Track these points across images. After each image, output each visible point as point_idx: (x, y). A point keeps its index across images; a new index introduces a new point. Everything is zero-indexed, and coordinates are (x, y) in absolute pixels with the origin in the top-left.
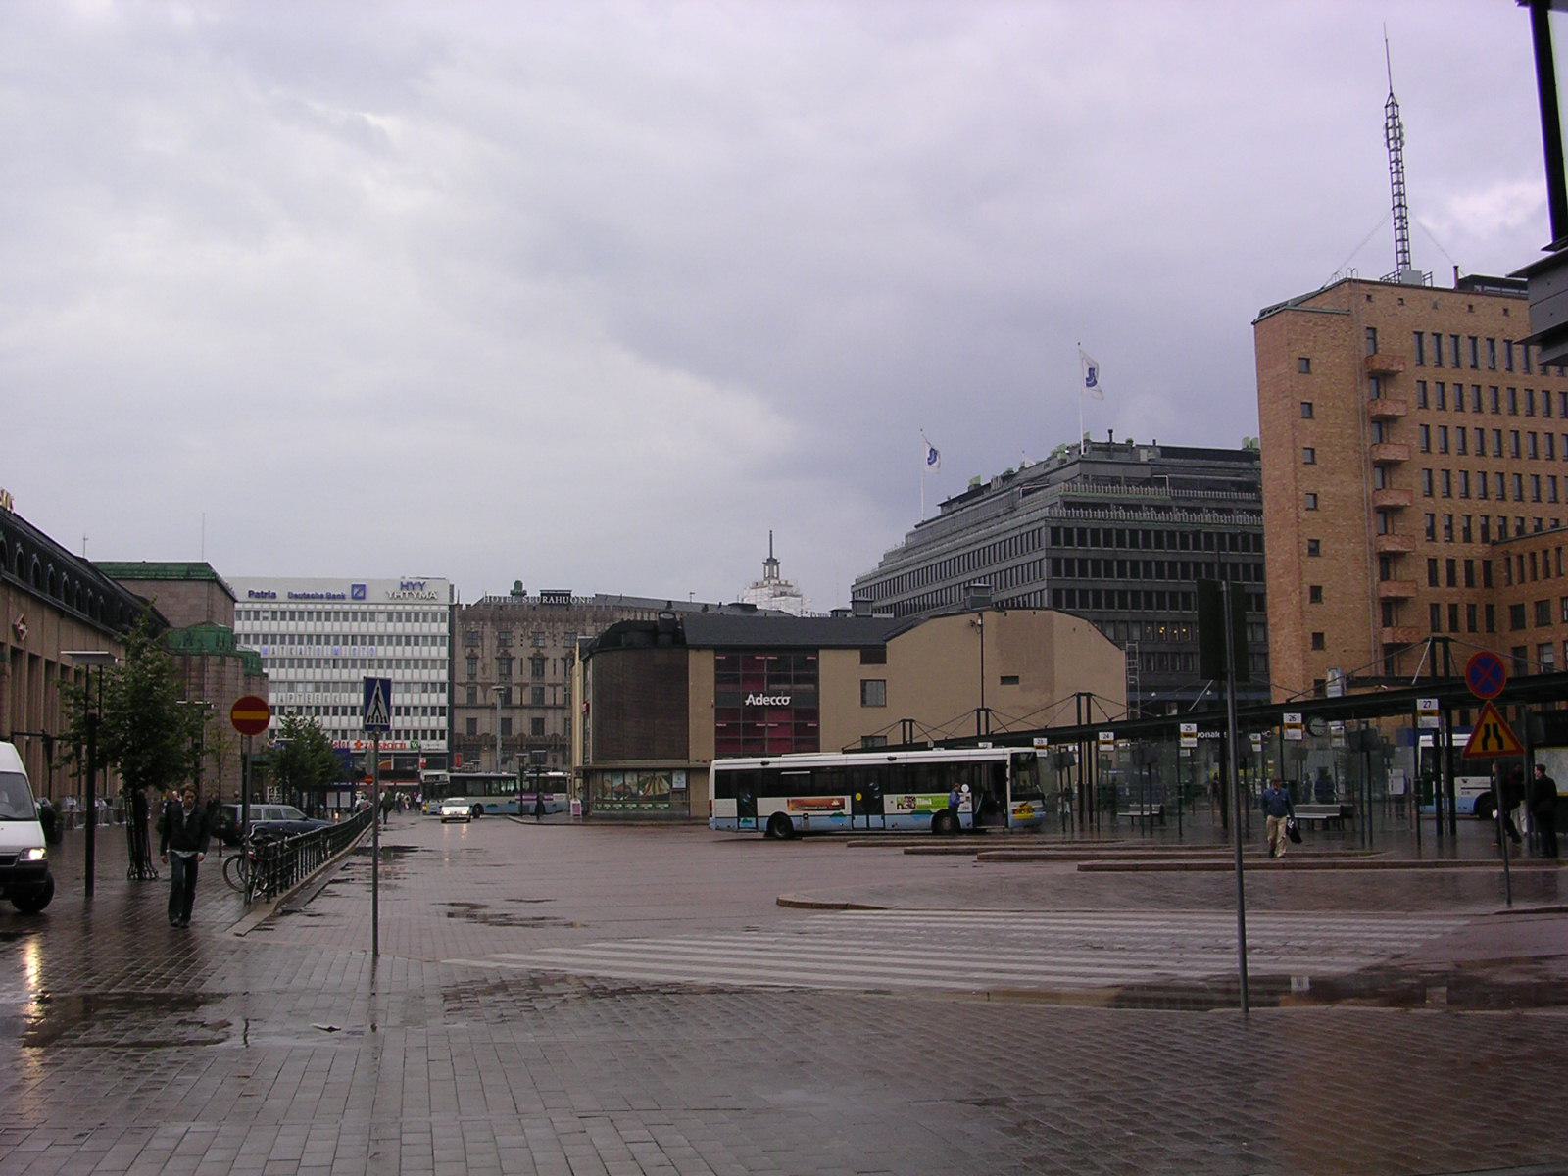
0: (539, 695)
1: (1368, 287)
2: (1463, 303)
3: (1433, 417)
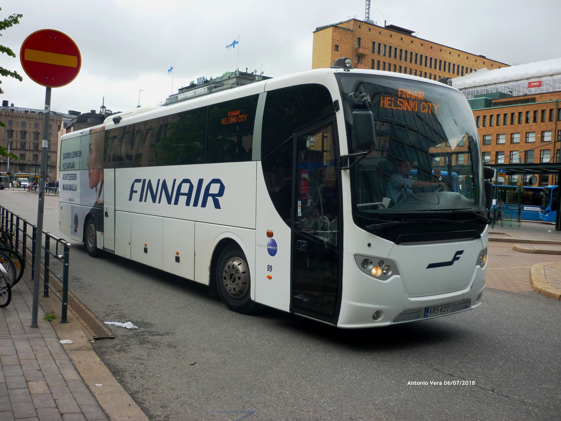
0: (23, 146)
1: (360, 23)
2: (389, 34)
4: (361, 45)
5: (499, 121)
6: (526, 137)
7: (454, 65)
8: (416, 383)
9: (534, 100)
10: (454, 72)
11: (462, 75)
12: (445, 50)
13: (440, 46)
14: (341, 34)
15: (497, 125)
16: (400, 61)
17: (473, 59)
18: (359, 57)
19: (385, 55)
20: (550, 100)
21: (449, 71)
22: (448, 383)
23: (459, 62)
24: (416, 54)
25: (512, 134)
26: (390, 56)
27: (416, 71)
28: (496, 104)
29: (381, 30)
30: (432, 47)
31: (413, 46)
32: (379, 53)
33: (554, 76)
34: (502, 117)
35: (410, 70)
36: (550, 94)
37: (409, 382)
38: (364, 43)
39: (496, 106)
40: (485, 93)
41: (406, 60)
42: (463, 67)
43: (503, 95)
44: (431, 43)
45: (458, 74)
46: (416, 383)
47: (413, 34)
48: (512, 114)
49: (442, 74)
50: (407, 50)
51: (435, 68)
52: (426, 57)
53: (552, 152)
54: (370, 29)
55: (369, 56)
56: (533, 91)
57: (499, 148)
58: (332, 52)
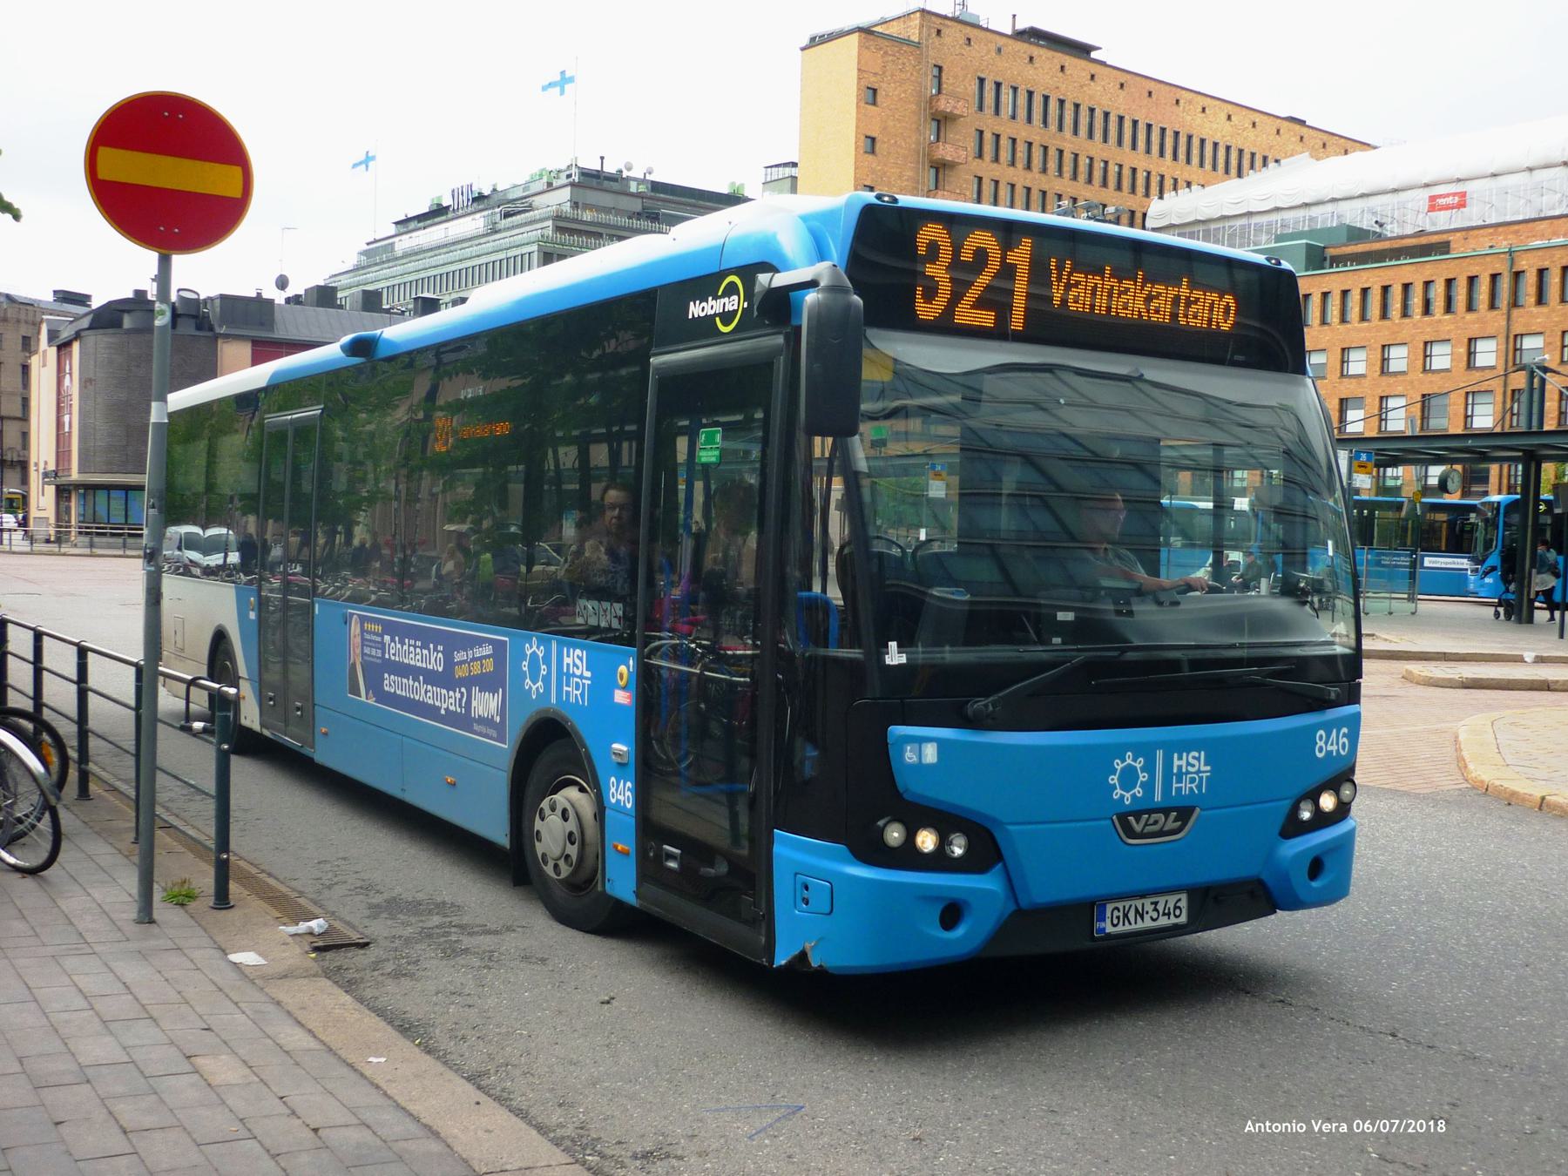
1: (939, 21)
2: (1025, 53)
3: (987, 169)
4: (944, 86)
5: (1349, 309)
6: (1426, 356)
7: (1216, 145)
8: (1270, 1128)
9: (1444, 247)
10: (1214, 168)
11: (1240, 175)
12: (1190, 102)
13: (1174, 89)
14: (886, 53)
15: (1343, 320)
16: (1058, 134)
17: (1272, 126)
18: (939, 121)
19: (1013, 117)
20: (1491, 247)
21: (1202, 165)
22: (1366, 1125)
23: (1229, 138)
24: (1106, 115)
25: (1384, 346)
26: (1029, 120)
27: (1106, 163)
28: (1337, 260)
29: (1001, 41)
30: (1150, 93)
31: (1096, 88)
32: (997, 112)
33: (1499, 178)
34: (1355, 297)
35: (1087, 161)
36: (1491, 230)
37: (1249, 1123)
38: (951, 81)
39: (1338, 266)
40: (1306, 228)
41: (1076, 132)
42: (1241, 151)
43: (1357, 234)
44: (1148, 81)
45: (1227, 171)
46: (1270, 1128)
47: (1094, 55)
48: (1385, 289)
49: (1181, 170)
50: (1078, 102)
51: (1162, 154)
52: (1135, 123)
53: (1499, 398)
54: (969, 40)
55: (968, 120)
56: (1443, 221)
57: (1348, 389)
58: (858, 107)
